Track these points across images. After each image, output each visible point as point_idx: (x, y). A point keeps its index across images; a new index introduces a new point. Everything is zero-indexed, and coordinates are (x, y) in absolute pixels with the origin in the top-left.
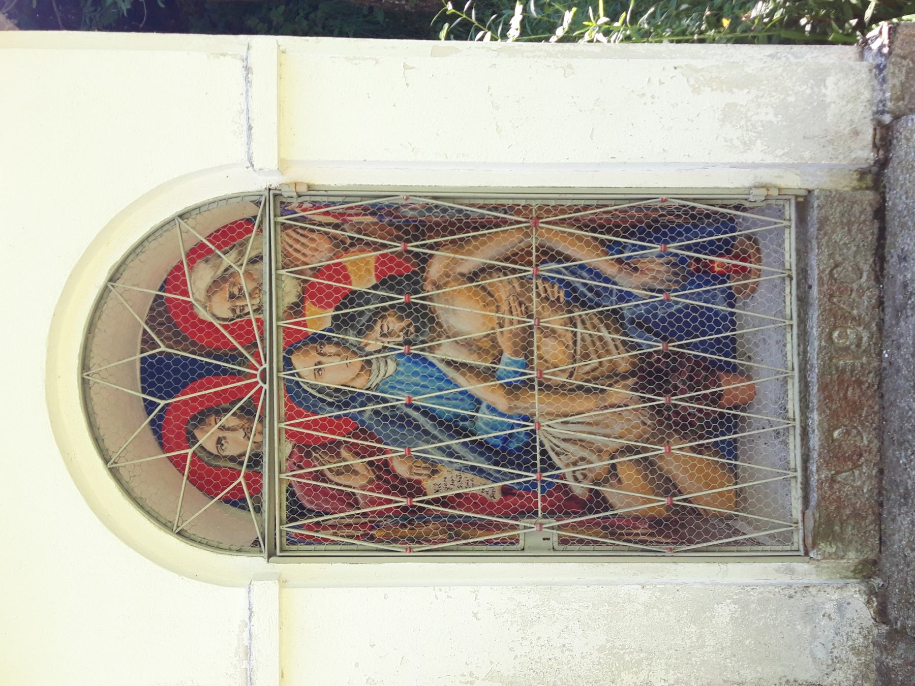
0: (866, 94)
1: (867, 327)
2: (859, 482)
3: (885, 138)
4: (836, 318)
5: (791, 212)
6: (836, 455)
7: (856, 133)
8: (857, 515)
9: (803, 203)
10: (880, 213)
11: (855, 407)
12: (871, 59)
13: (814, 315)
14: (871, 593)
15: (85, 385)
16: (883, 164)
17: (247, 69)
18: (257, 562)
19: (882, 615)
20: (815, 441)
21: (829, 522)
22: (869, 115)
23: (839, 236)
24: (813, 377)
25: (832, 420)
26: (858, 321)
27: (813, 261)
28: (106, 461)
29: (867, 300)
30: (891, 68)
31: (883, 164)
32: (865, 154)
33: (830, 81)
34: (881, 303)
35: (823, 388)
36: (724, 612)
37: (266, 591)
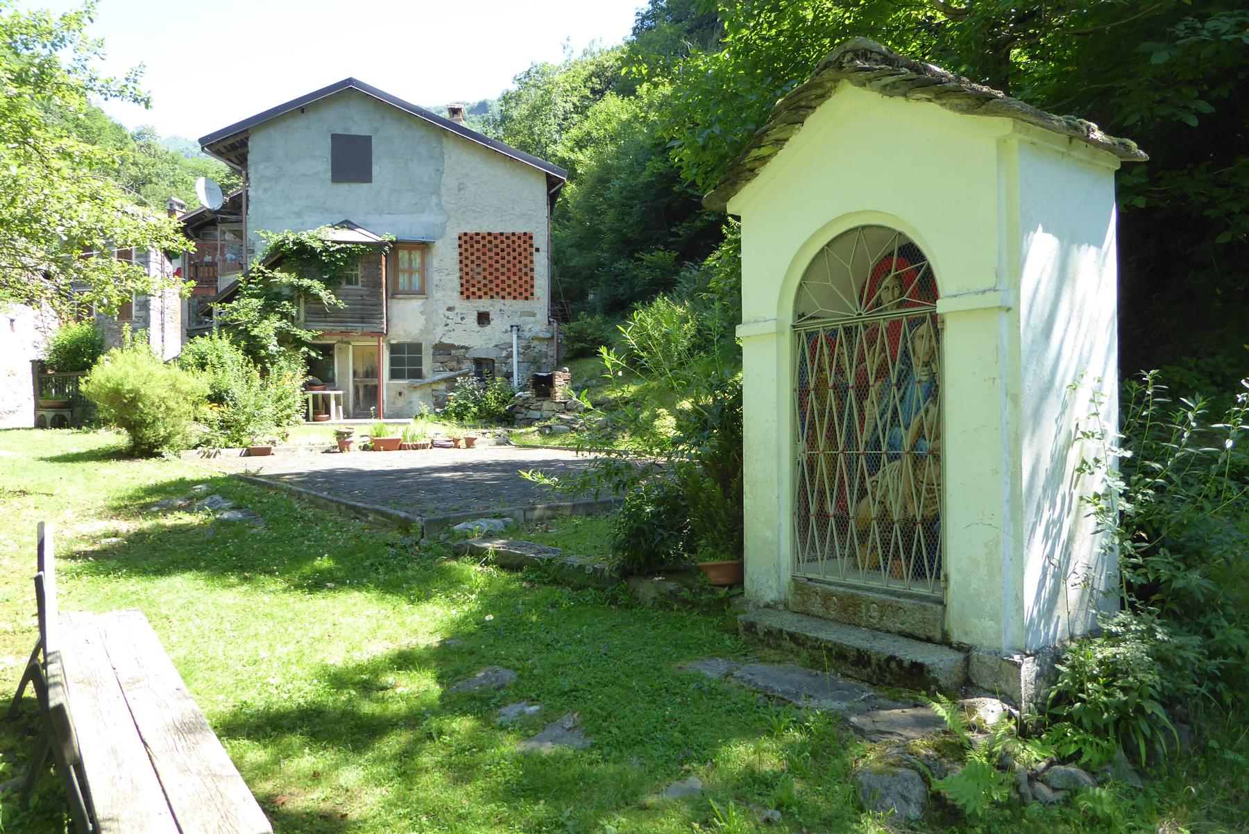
0: (986, 644)
1: (878, 623)
2: (817, 608)
3: (964, 649)
4: (883, 607)
5: (938, 594)
6: (827, 597)
7: (966, 634)
8: (804, 602)
9: (941, 602)
10: (929, 640)
11: (845, 610)
12: (1005, 651)
13: (883, 597)
14: (776, 603)
15: (856, 229)
16: (950, 645)
17: (984, 292)
18: (789, 318)
19: (767, 606)
20: (832, 588)
21: (802, 589)
22: (975, 643)
23: (918, 616)
24: (859, 592)
25: (841, 599)
26: (881, 619)
27: (912, 601)
28: (828, 245)
29: (890, 625)
30: (994, 658)
31: (950, 645)
32: (956, 637)
33: (992, 623)
34: (889, 632)
35: (852, 596)
36: (769, 533)
37: (772, 327)
